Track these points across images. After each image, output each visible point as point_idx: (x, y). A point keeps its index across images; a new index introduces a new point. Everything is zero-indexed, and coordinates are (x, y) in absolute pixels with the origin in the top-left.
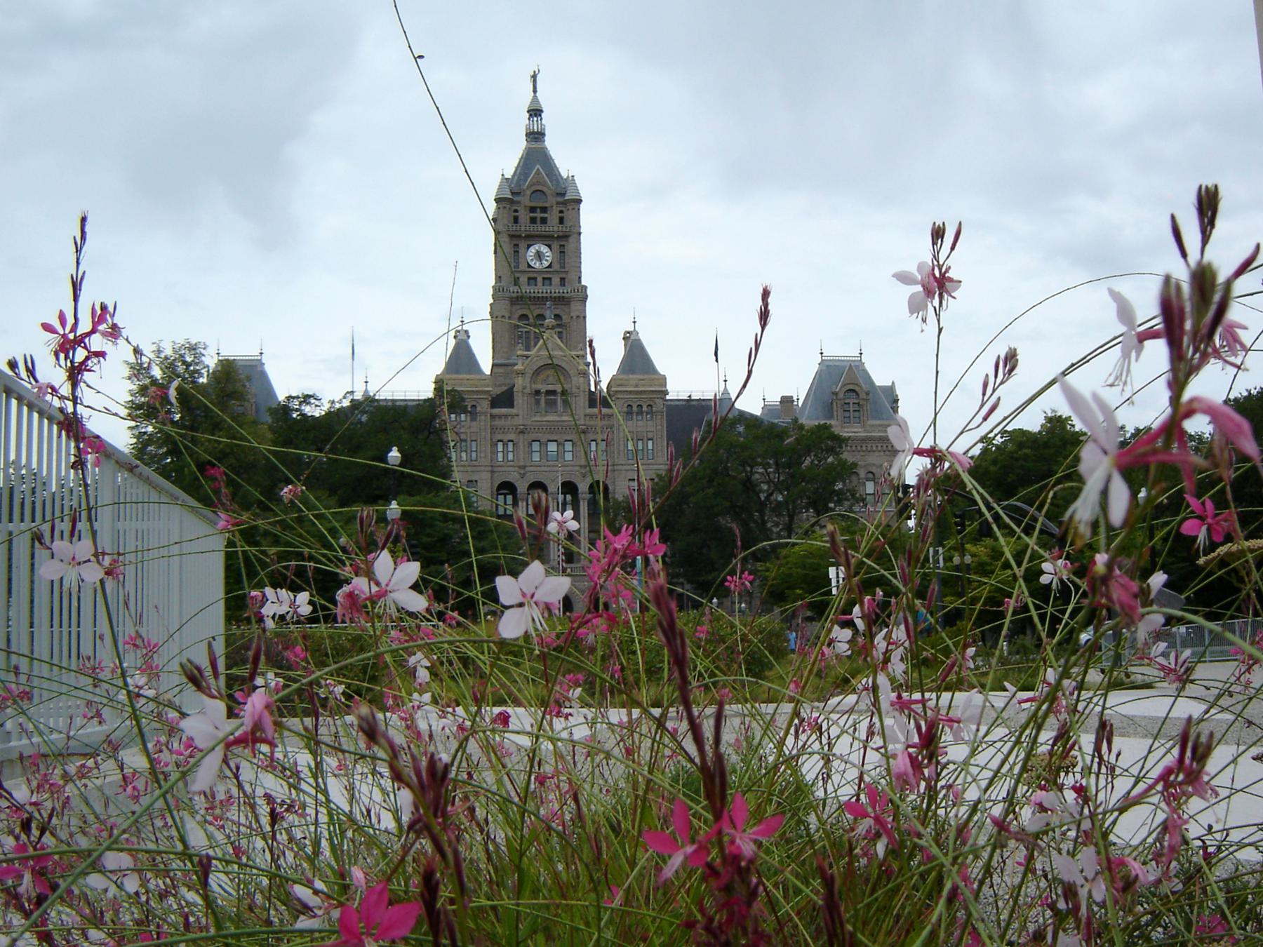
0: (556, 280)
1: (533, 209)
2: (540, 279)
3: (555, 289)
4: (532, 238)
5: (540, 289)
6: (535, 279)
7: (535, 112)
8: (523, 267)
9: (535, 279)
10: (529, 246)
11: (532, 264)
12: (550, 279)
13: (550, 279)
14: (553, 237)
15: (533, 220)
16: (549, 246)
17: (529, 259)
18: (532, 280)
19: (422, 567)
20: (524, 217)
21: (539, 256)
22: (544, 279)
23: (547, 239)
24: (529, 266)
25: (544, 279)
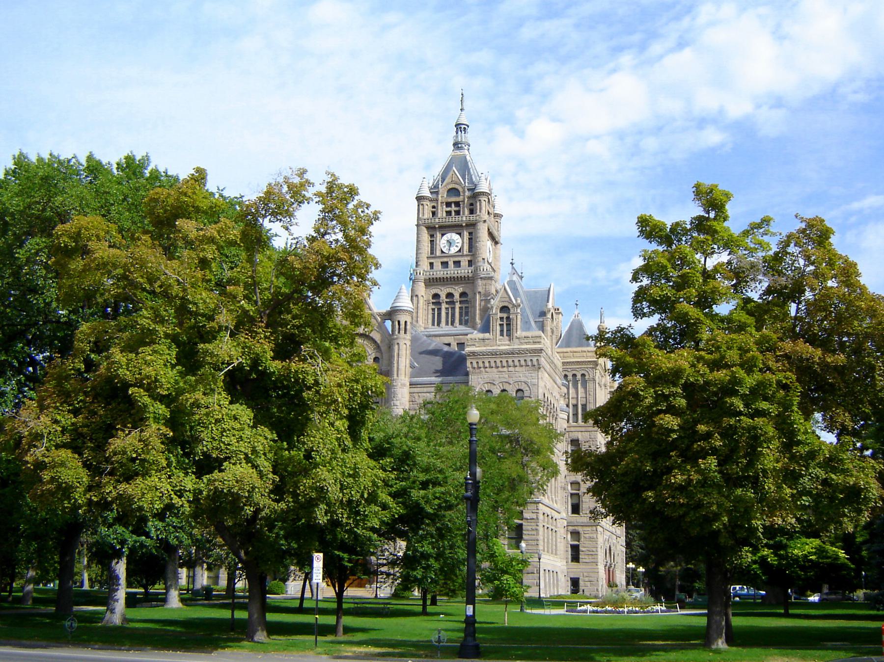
0: (464, 262)
1: (448, 204)
2: (451, 264)
3: (465, 270)
4: (445, 229)
5: (452, 271)
6: (447, 263)
7: (460, 127)
8: (438, 253)
9: (447, 263)
10: (443, 235)
11: (444, 250)
12: (459, 262)
13: (459, 262)
14: (461, 226)
15: (449, 213)
16: (460, 234)
17: (442, 246)
18: (445, 264)
19: (187, 568)
20: (442, 212)
21: (450, 243)
22: (455, 262)
23: (457, 228)
24: (442, 252)
25: (455, 262)
